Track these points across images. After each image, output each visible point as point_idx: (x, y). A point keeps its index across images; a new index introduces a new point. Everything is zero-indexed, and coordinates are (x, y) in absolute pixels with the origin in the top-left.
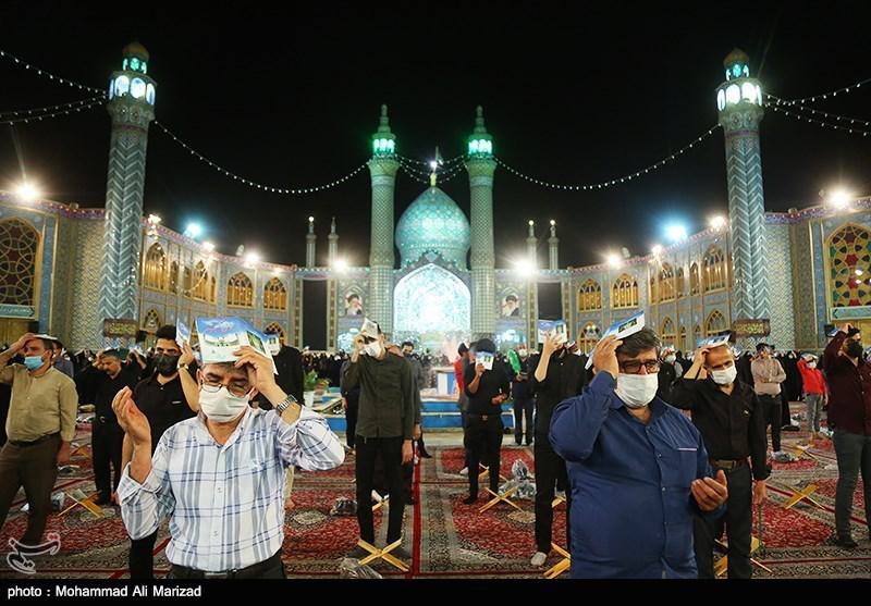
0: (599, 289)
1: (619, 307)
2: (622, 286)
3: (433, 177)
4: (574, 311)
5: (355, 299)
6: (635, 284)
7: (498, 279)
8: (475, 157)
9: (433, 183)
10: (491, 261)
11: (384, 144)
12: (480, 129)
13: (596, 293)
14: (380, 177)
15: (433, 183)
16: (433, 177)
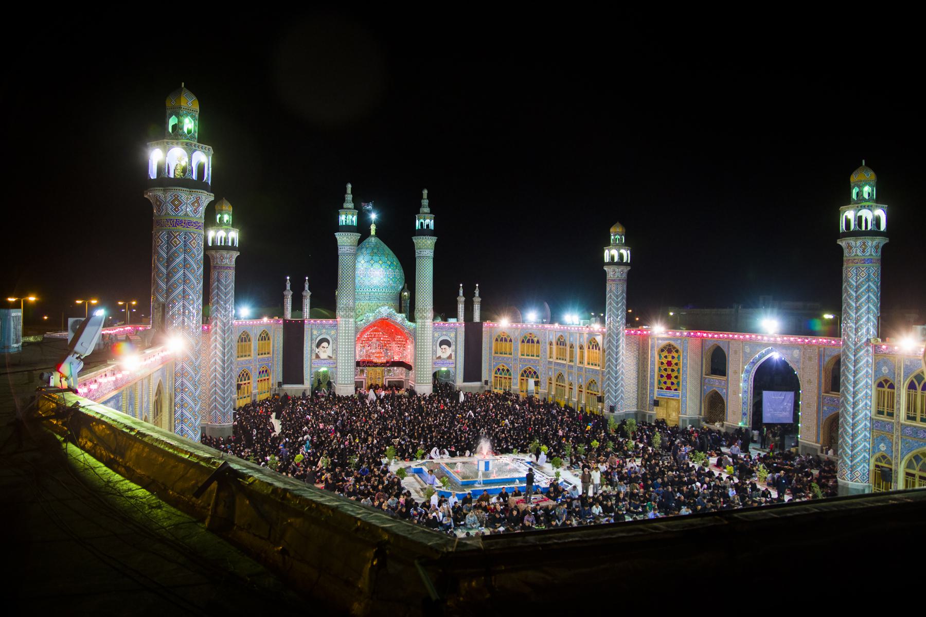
0: (511, 341)
1: (526, 357)
2: (528, 342)
3: (373, 228)
4: (490, 353)
5: (325, 344)
6: (538, 342)
7: (435, 329)
8: (424, 232)
9: (373, 233)
10: (430, 314)
11: (347, 218)
12: (427, 210)
13: (508, 343)
14: (345, 241)
15: (373, 233)
16: (373, 228)
